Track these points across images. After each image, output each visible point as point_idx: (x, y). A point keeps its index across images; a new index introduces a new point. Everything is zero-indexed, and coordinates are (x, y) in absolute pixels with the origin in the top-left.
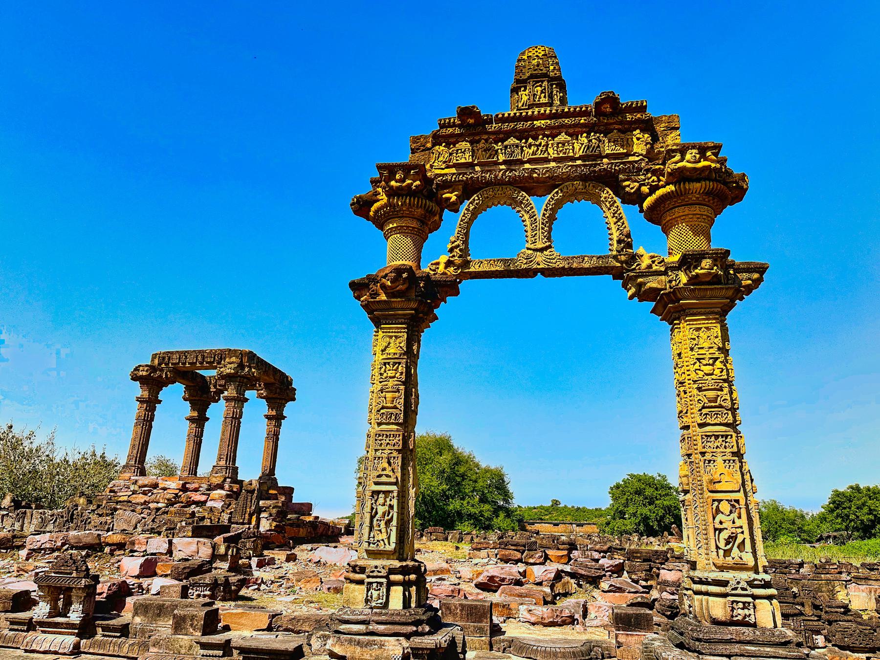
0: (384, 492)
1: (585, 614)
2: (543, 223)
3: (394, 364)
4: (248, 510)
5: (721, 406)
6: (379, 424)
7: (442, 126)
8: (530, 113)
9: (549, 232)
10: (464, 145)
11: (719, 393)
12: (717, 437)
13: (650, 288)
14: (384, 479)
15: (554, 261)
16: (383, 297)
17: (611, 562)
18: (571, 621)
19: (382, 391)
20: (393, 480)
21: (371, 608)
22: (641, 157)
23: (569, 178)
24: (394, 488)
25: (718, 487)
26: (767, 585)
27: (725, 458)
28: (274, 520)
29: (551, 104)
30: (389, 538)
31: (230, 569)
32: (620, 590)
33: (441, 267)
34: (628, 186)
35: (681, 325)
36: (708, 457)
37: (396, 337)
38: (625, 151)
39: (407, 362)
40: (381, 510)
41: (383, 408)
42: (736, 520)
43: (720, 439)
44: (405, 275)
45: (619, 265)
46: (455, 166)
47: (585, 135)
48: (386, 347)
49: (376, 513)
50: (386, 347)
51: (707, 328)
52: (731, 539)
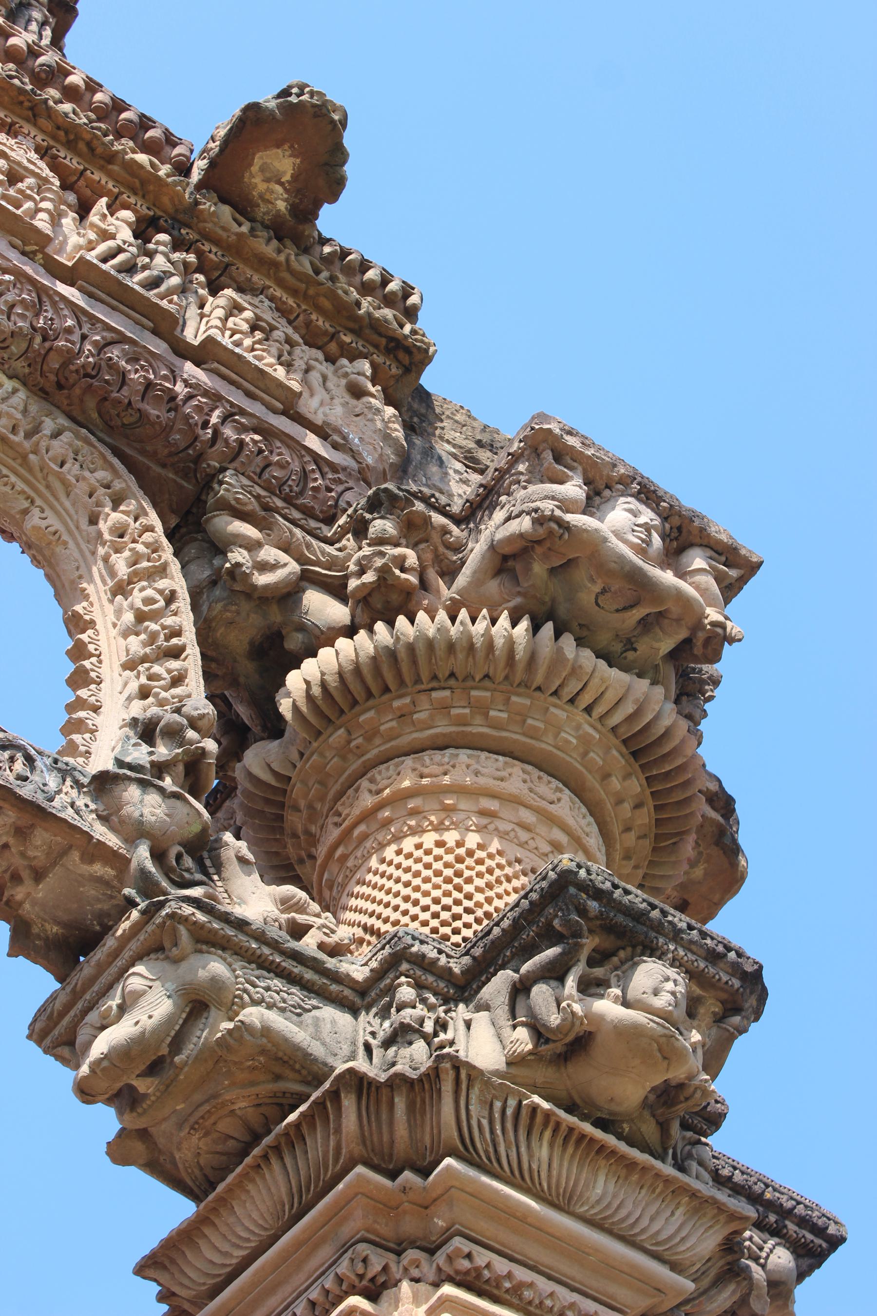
13: (266, 1031)
34: (252, 546)
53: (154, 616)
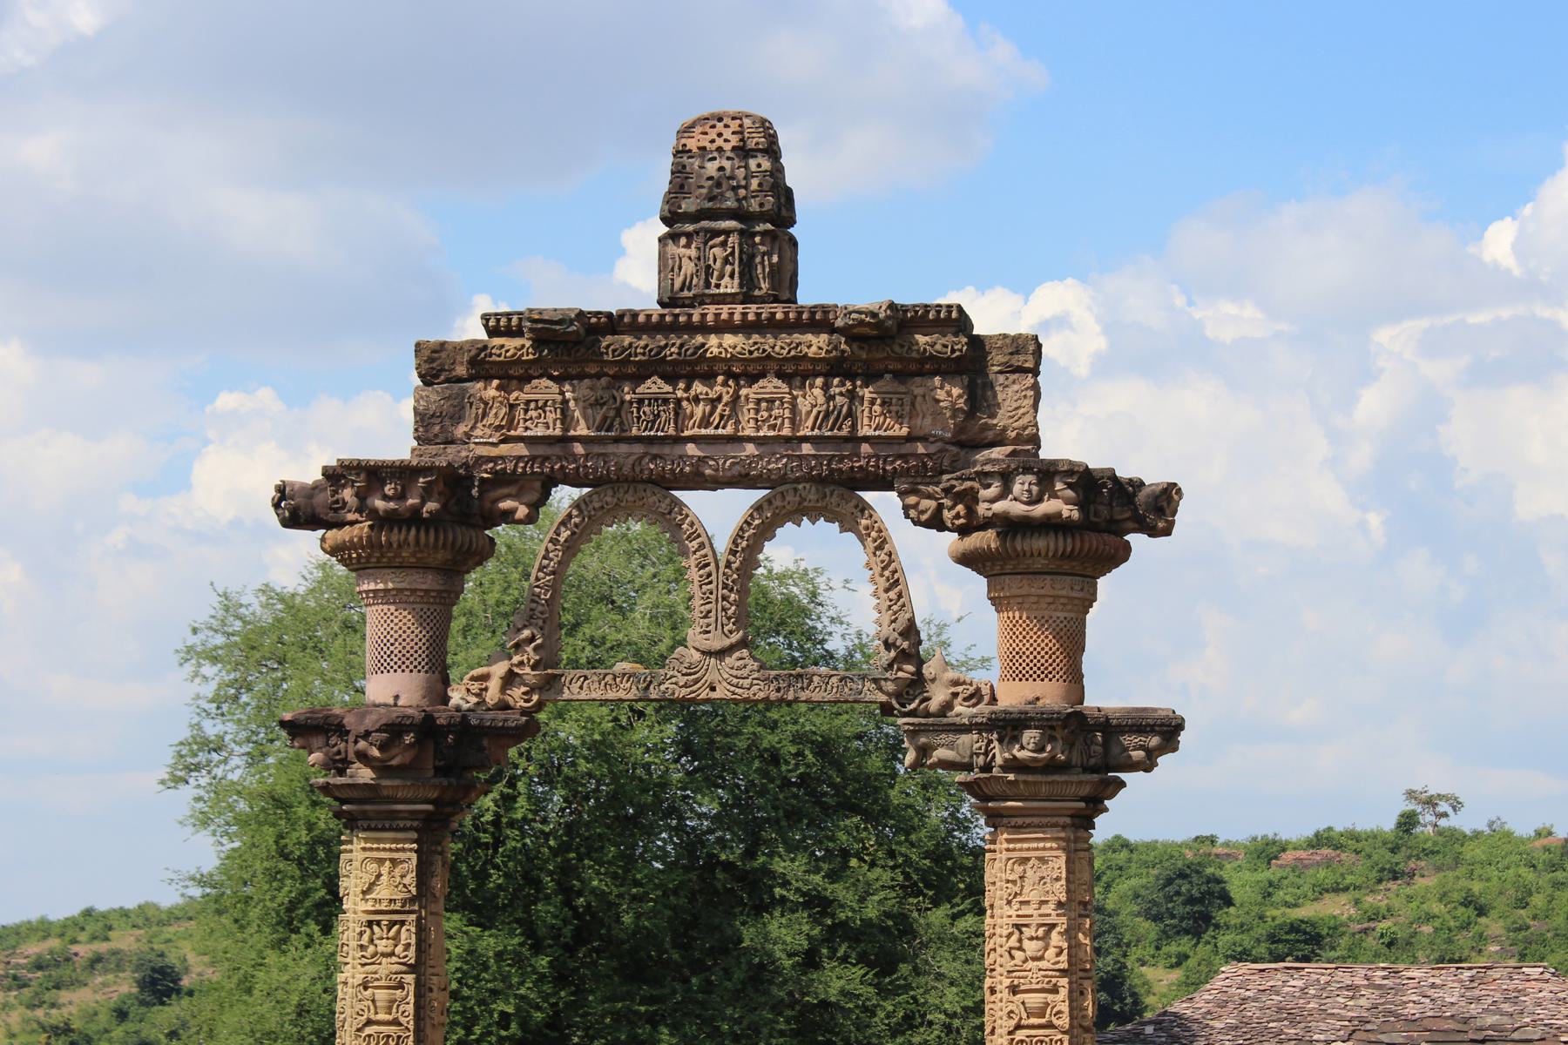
3: (392, 924)
5: (1050, 1025)
7: (492, 332)
8: (696, 318)
10: (544, 389)
11: (1050, 997)
15: (746, 683)
16: (364, 774)
22: (939, 444)
29: (747, 298)
33: (494, 685)
37: (393, 861)
38: (904, 431)
39: (419, 919)
41: (369, 1022)
44: (408, 739)
48: (372, 884)
50: (372, 884)
51: (1042, 860)
53: (884, 569)
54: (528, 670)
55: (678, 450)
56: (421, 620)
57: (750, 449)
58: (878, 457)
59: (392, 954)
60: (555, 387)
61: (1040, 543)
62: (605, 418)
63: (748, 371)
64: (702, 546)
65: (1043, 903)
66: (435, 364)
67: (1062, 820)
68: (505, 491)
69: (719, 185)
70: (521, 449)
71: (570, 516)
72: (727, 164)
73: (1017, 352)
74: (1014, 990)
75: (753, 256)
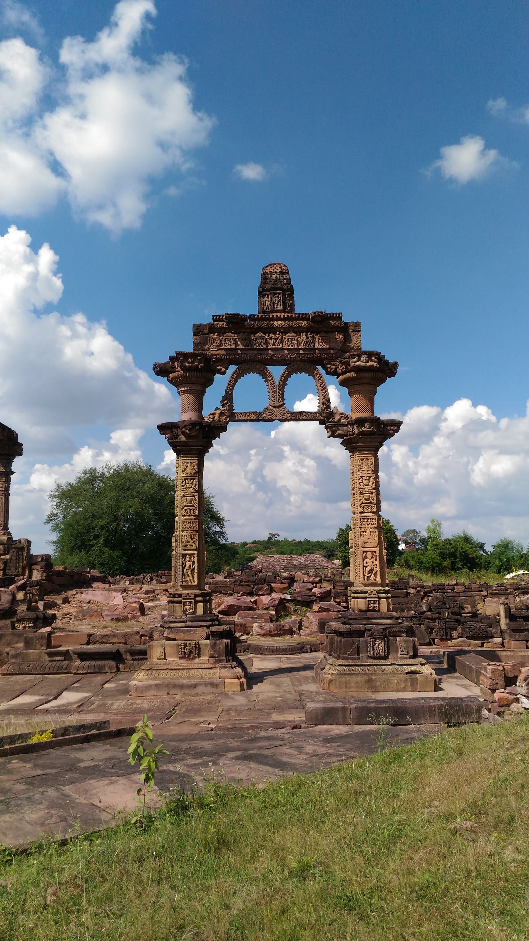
0: (189, 554)
1: (300, 628)
2: (279, 389)
4: (21, 564)
5: (371, 503)
6: (183, 516)
7: (214, 320)
9: (283, 394)
10: (230, 335)
12: (368, 519)
14: (189, 547)
16: (183, 438)
17: (320, 590)
18: (291, 632)
19: (184, 496)
20: (194, 548)
21: (186, 615)
23: (295, 360)
24: (195, 552)
25: (367, 545)
26: (386, 592)
27: (371, 530)
28: (44, 571)
29: (284, 311)
30: (193, 579)
31: (28, 609)
32: (327, 610)
33: (217, 416)
34: (330, 368)
35: (354, 456)
36: (363, 530)
40: (188, 564)
41: (185, 506)
42: (374, 561)
43: (369, 520)
44: (197, 427)
45: (323, 418)
46: (224, 349)
47: (304, 333)
48: (185, 469)
49: (185, 566)
50: (185, 469)
52: (371, 571)
54: (226, 411)
55: (266, 352)
56: (196, 398)
57: (286, 352)
58: (320, 354)
59: (191, 487)
60: (233, 335)
61: (367, 375)
62: (247, 343)
63: (284, 331)
64: (272, 379)
65: (368, 470)
66: (198, 330)
67: (373, 449)
68: (218, 364)
69: (276, 281)
70: (224, 352)
71: (236, 371)
72: (278, 276)
73: (356, 326)
74: (361, 493)
75: (285, 301)
